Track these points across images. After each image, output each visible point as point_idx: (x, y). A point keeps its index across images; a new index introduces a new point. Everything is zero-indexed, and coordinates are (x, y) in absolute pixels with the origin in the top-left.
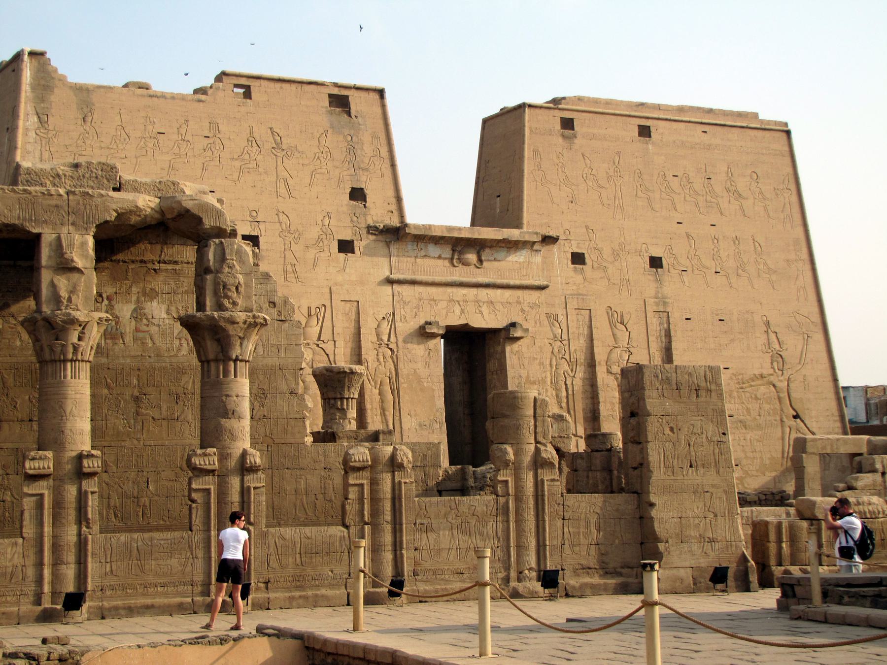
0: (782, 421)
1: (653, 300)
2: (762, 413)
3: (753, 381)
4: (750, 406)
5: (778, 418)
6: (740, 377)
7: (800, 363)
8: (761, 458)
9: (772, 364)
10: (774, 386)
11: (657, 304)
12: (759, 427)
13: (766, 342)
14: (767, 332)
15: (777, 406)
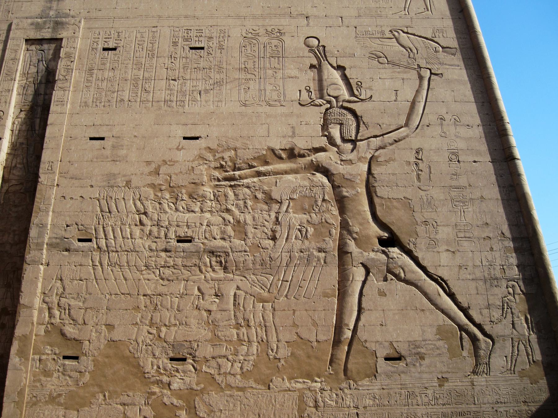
0: (343, 252)
1: (30, 21)
2: (282, 233)
3: (266, 163)
4: (249, 218)
5: (332, 245)
6: (226, 155)
7: (407, 125)
8: (264, 343)
9: (325, 126)
10: (326, 172)
11: (38, 27)
12: (267, 265)
13: (313, 86)
14: (317, 68)
15: (333, 214)
